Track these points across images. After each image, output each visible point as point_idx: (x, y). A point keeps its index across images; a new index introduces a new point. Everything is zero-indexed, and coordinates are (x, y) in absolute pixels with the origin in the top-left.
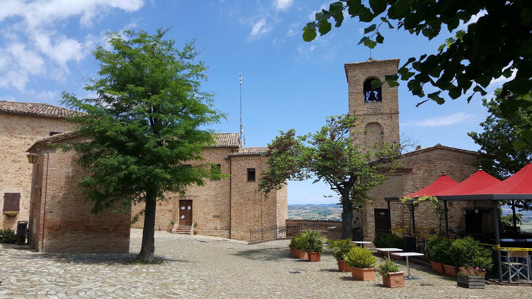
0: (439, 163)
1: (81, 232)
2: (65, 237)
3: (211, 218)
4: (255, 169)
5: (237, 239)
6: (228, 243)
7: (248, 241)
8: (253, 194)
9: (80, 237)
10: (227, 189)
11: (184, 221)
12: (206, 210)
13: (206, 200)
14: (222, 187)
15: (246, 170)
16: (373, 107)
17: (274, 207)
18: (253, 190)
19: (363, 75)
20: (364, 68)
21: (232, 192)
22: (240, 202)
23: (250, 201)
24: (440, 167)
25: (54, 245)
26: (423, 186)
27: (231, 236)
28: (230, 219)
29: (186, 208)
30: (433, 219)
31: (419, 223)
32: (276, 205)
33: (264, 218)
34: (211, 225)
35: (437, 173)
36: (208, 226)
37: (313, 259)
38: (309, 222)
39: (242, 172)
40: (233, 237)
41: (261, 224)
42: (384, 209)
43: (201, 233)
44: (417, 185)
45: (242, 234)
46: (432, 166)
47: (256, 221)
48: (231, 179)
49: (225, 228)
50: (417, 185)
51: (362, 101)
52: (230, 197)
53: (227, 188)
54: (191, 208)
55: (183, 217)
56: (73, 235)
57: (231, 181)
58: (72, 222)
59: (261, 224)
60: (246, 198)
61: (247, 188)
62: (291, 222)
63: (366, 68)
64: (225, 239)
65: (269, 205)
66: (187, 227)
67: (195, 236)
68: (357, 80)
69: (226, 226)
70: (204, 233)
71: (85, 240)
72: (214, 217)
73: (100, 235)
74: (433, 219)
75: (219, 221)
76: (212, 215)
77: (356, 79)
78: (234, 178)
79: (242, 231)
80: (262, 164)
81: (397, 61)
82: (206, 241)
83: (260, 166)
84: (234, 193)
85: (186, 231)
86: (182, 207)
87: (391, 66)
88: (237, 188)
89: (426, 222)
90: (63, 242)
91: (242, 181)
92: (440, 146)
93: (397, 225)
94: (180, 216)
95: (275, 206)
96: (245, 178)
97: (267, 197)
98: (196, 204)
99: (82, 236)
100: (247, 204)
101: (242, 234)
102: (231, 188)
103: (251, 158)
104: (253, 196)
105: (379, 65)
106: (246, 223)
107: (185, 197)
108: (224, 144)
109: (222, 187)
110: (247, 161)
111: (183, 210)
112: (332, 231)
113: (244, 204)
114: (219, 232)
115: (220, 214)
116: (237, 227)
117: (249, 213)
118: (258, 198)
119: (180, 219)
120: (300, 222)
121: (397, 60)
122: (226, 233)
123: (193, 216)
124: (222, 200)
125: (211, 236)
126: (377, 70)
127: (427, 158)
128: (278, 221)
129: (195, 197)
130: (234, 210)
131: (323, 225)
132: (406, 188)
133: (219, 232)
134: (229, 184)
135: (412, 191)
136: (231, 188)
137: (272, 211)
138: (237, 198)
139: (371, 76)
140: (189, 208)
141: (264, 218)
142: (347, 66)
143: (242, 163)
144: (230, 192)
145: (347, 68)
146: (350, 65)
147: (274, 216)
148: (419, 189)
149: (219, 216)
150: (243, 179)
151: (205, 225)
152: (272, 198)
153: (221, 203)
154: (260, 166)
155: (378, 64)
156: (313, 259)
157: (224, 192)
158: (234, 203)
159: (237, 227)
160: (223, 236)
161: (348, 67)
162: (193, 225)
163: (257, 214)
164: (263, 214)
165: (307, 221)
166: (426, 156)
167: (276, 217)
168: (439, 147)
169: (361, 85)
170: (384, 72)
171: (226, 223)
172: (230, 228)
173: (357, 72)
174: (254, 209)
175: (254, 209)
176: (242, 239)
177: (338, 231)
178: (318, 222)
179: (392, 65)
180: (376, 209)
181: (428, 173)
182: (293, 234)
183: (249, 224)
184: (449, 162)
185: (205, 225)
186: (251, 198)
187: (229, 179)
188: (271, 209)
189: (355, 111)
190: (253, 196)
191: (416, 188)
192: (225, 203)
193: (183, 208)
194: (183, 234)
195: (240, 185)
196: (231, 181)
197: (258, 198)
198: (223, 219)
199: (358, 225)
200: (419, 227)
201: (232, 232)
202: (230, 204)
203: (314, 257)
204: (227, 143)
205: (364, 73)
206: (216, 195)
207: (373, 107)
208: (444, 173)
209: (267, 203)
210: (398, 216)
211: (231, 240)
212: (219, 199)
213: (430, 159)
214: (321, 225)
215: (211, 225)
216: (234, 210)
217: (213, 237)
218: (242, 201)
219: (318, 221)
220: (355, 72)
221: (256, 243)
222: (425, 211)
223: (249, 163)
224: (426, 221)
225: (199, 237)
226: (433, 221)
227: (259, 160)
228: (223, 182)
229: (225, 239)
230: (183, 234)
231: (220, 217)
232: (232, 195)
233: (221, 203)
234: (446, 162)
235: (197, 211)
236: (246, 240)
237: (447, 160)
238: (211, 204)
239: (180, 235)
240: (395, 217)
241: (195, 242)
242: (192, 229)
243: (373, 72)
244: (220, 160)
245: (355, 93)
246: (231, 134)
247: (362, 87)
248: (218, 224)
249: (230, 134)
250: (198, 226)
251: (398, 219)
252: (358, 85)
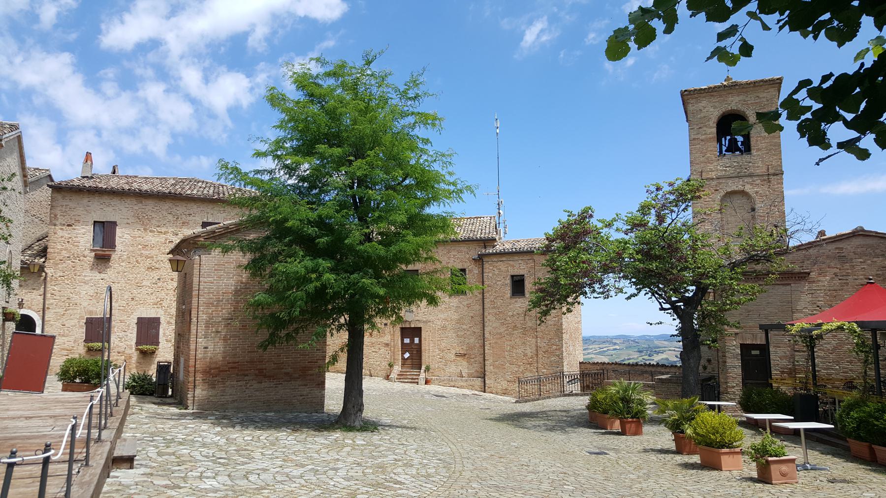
0: (861, 262)
1: (251, 378)
2: (227, 387)
3: (453, 357)
4: (523, 276)
5: (497, 393)
6: (482, 400)
7: (515, 397)
8: (521, 318)
9: (250, 386)
10: (478, 309)
11: (409, 362)
12: (443, 344)
13: (444, 328)
14: (468, 306)
15: (509, 277)
16: (735, 164)
17: (559, 341)
18: (521, 311)
19: (715, 107)
20: (716, 96)
21: (486, 314)
22: (499, 331)
23: (516, 330)
24: (864, 268)
25: (211, 398)
26: (830, 303)
27: (486, 388)
28: (484, 360)
29: (412, 341)
30: (851, 362)
31: (825, 369)
32: (562, 337)
33: (542, 359)
34: (453, 369)
35: (856, 279)
36: (447, 370)
37: (629, 431)
38: (621, 367)
39: (503, 281)
40: (489, 390)
41: (537, 368)
42: (757, 344)
43: (436, 382)
44: (819, 301)
45: (504, 384)
46: (848, 267)
47: (528, 364)
48: (483, 294)
49: (475, 374)
50: (819, 301)
51: (714, 155)
52: (483, 324)
53: (478, 307)
54: (420, 341)
55: (407, 355)
56: (239, 383)
57: (483, 296)
58: (238, 363)
59: (537, 368)
60: (510, 325)
61: (511, 309)
62: (588, 366)
63: (721, 96)
64: (476, 392)
65: (549, 337)
66: (415, 372)
67: (428, 387)
68: (705, 117)
69: (476, 371)
70: (441, 382)
71: (257, 391)
72: (457, 355)
73: (279, 384)
74: (851, 363)
75: (465, 363)
76: (454, 352)
77: (702, 115)
78: (488, 291)
79: (505, 380)
80: (536, 267)
81: (778, 81)
82: (444, 395)
83: (532, 271)
84: (489, 317)
85: (412, 379)
86: (405, 339)
87: (766, 91)
88: (494, 308)
89: (837, 367)
90: (224, 394)
91: (502, 296)
92: (862, 230)
93: (783, 372)
94: (403, 354)
95: (561, 339)
96: (508, 291)
97: (543, 322)
98: (427, 333)
99: (252, 386)
100: (511, 334)
101: (504, 384)
102: (483, 309)
103: (516, 258)
104: (521, 322)
105: (744, 90)
107: (410, 322)
108: (471, 235)
109: (468, 306)
110: (511, 263)
111: (407, 344)
112: (663, 383)
113: (507, 334)
114: (466, 381)
115: (467, 350)
116: (496, 373)
118: (530, 325)
119: (403, 358)
120: (605, 366)
121: (778, 79)
122: (478, 382)
123: (423, 353)
124: (470, 327)
125: (454, 386)
126: (741, 97)
127: (838, 253)
128: (565, 363)
129: (426, 322)
130: (490, 344)
131: (646, 372)
132: (799, 308)
133: (466, 381)
134: (481, 301)
135: (811, 312)
136: (483, 309)
137: (554, 347)
138: (494, 325)
139: (730, 109)
140: (416, 340)
141: (542, 359)
142: (686, 93)
143: (502, 266)
144: (483, 314)
145: (685, 98)
146: (692, 93)
147: (558, 356)
148: (823, 308)
149: (465, 355)
150: (504, 293)
151: (443, 369)
152: (555, 325)
153: (468, 333)
154: (532, 271)
155: (743, 88)
156: (629, 431)
157: (472, 315)
158: (490, 333)
159: (496, 373)
160: (472, 387)
161: (687, 95)
162: (423, 368)
163: (529, 352)
164: (540, 352)
165: (617, 365)
166: (836, 248)
167: (562, 357)
168: (861, 233)
169: (711, 125)
170: (753, 102)
171: (477, 367)
172: (485, 375)
173: (704, 103)
174: (524, 343)
175: (524, 343)
176: (505, 394)
177: (675, 383)
178: (638, 367)
179: (768, 89)
180: (744, 344)
181: (840, 280)
182: (592, 387)
184: (881, 259)
185: (443, 369)
186: (518, 325)
187: (480, 293)
188: (553, 344)
189: (702, 172)
190: (521, 322)
191: (818, 306)
192: (475, 332)
193: (407, 341)
194: (407, 382)
195: (499, 302)
196: (483, 296)
197: (530, 324)
198: (473, 360)
199: (710, 373)
200: (824, 375)
201: (487, 382)
202: (484, 334)
203: (631, 427)
204: (475, 233)
205: (717, 104)
206: (459, 320)
207: (735, 164)
208: (871, 279)
209: (546, 333)
210: (785, 357)
211: (487, 395)
212: (464, 327)
213: (843, 255)
214: (643, 373)
215: (453, 369)
216: (490, 344)
217: (457, 389)
218: (502, 330)
219: (637, 364)
220: (700, 104)
221: (529, 401)
222: (835, 348)
223: (513, 266)
224: (837, 365)
225: (433, 388)
226: (850, 366)
227: (531, 261)
228: (471, 298)
229: (476, 392)
230: (407, 382)
231: (467, 356)
232: (486, 320)
233: (468, 333)
234: (875, 259)
235: (429, 346)
236: (512, 394)
237: (877, 256)
238: (451, 334)
239: (403, 384)
240: (779, 359)
241: (427, 396)
242: (423, 375)
243: (734, 103)
244: (466, 262)
245: (702, 140)
246: (482, 219)
247: (714, 130)
248: (463, 367)
249: (480, 218)
250: (431, 371)
251: (785, 362)
252: (706, 126)
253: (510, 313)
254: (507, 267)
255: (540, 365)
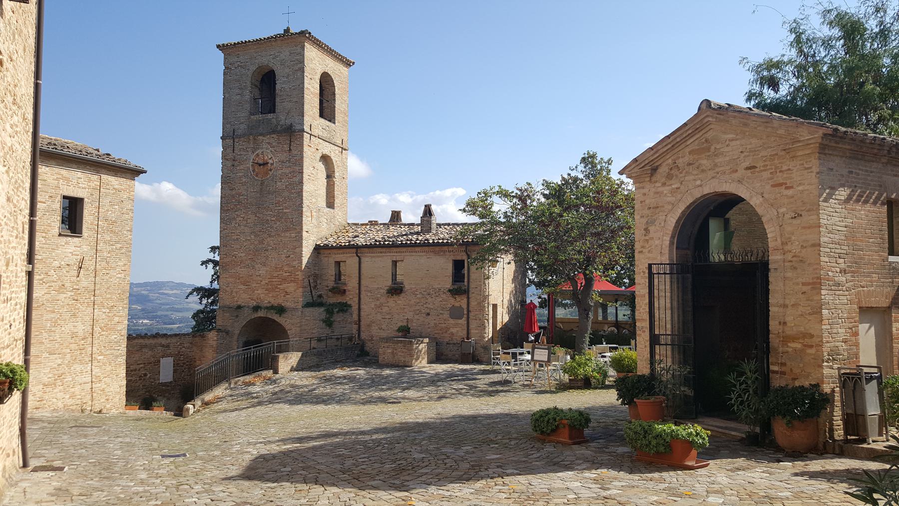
15: (59, 198)
18: (74, 260)
60: (53, 284)
106: (52, 357)
117: (58, 330)
137: (116, 319)
164: (97, 329)
175: (74, 315)
183: (59, 361)
209: (108, 296)
223: (67, 180)
253: (56, 264)
254: (57, 179)
255: (94, 349)
